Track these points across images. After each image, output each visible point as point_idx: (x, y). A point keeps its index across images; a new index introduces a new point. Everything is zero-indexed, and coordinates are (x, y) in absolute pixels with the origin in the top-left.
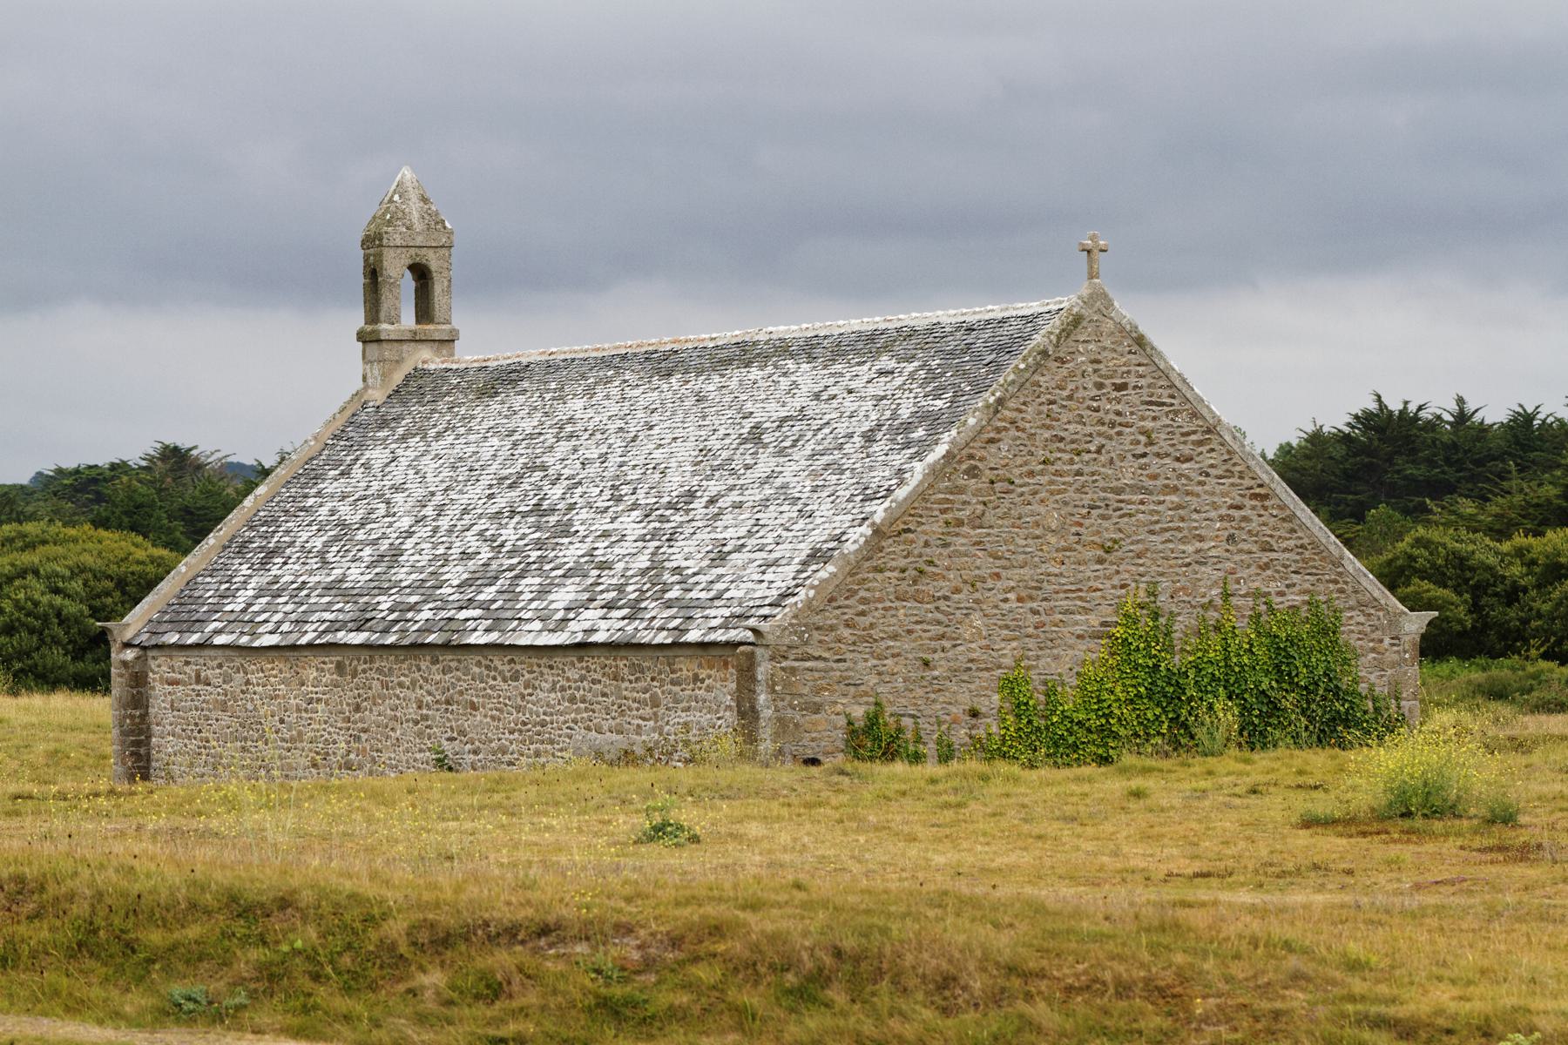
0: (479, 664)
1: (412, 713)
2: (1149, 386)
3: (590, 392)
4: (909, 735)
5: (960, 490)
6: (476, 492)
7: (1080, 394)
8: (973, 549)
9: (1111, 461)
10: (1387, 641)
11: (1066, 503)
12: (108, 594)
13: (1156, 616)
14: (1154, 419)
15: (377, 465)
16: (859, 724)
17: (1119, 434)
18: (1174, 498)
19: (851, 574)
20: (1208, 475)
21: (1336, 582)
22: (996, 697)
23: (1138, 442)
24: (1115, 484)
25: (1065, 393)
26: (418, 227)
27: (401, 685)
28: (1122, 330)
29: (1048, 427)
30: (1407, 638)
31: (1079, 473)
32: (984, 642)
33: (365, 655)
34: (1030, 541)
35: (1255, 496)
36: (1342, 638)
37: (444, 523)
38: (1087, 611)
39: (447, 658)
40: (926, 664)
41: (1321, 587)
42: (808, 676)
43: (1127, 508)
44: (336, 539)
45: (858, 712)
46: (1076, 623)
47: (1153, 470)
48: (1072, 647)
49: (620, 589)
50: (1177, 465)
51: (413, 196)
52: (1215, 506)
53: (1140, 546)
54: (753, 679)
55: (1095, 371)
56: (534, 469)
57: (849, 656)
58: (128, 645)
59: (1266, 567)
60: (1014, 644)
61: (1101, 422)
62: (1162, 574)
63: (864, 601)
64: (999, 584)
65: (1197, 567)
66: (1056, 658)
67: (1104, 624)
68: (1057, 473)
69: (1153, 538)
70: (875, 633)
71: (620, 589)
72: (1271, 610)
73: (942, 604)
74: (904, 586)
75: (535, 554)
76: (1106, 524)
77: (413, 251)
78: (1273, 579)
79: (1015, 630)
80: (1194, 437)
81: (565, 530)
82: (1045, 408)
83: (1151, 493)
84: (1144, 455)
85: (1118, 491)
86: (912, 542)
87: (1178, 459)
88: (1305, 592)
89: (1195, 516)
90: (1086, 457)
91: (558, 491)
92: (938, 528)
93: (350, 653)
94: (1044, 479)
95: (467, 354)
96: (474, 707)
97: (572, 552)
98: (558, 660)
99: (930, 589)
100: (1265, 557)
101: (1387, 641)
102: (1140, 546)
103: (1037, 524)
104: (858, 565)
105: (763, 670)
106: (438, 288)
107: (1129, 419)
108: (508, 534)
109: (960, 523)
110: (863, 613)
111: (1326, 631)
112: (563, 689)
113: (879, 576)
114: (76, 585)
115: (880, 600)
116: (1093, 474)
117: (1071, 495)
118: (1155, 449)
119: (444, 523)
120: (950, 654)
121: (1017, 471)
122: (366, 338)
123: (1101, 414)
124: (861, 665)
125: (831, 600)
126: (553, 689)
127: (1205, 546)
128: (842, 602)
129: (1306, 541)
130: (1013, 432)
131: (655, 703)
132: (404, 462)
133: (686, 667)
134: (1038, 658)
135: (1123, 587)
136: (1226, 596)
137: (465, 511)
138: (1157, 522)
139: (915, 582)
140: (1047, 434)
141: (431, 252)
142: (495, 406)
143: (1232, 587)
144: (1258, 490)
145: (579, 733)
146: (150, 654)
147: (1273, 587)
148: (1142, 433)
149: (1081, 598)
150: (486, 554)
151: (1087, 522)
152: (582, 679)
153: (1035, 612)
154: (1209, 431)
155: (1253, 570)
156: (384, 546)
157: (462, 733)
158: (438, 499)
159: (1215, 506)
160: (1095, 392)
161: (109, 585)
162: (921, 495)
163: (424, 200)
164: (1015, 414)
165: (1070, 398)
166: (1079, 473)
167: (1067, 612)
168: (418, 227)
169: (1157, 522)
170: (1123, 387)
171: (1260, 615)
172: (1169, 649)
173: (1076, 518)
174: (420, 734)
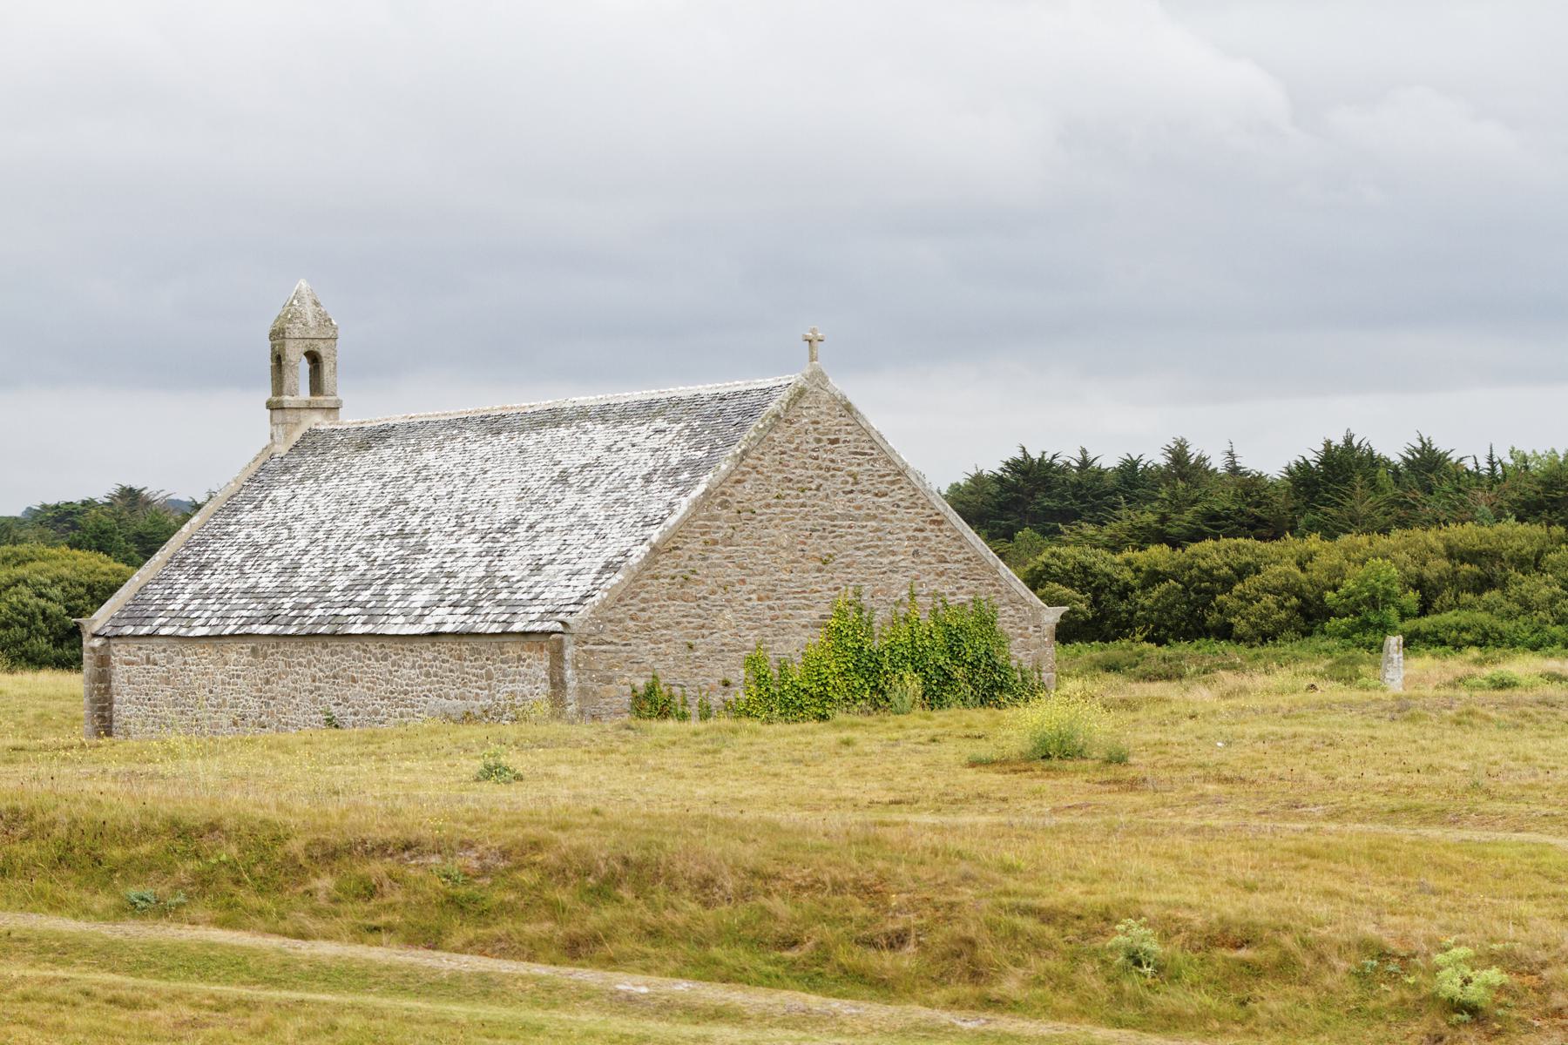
0: (358, 648)
1: (308, 684)
3: (440, 446)
4: (678, 700)
5: (716, 518)
6: (355, 521)
7: (805, 446)
8: (725, 562)
10: (1031, 629)
12: (80, 597)
13: (860, 611)
15: (281, 501)
16: (641, 692)
18: (874, 524)
19: (635, 580)
22: (742, 672)
26: (312, 323)
27: (300, 664)
28: (835, 399)
31: (803, 505)
33: (273, 641)
35: (933, 522)
36: (998, 627)
37: (332, 544)
39: (334, 643)
40: (691, 647)
41: (982, 589)
42: (603, 656)
43: (839, 531)
44: (251, 556)
45: (640, 683)
49: (463, 592)
52: (904, 529)
54: (562, 659)
56: (399, 503)
58: (95, 635)
59: (942, 574)
63: (644, 600)
64: (744, 588)
66: (787, 642)
67: (822, 617)
70: (653, 624)
71: (463, 592)
72: (946, 607)
73: (702, 602)
74: (673, 590)
75: (399, 567)
76: (823, 543)
79: (756, 623)
81: (422, 549)
85: (832, 518)
90: (809, 493)
91: (416, 520)
92: (699, 546)
93: (261, 641)
94: (778, 510)
95: (349, 418)
96: (354, 680)
97: (426, 565)
98: (417, 645)
101: (1031, 629)
103: (773, 543)
104: (640, 574)
105: (570, 652)
106: (326, 369)
107: (840, 465)
108: (379, 552)
109: (715, 543)
110: (643, 610)
111: (986, 622)
112: (420, 667)
113: (655, 582)
114: (56, 592)
115: (656, 600)
117: (797, 521)
118: (859, 487)
119: (332, 544)
122: (273, 407)
124: (642, 648)
126: (413, 667)
127: (897, 559)
128: (627, 601)
130: (754, 475)
131: (489, 677)
132: (301, 499)
133: (512, 650)
136: (913, 596)
137: (347, 535)
140: (780, 477)
142: (369, 456)
143: (917, 589)
145: (433, 699)
146: (112, 642)
147: (947, 589)
150: (363, 567)
152: (435, 659)
155: (932, 576)
156: (287, 561)
157: (346, 700)
158: (327, 525)
159: (904, 529)
160: (815, 445)
161: (82, 590)
162: (686, 522)
163: (316, 304)
165: (796, 449)
166: (803, 505)
168: (312, 323)
170: (833, 442)
172: (871, 635)
173: (802, 539)
174: (314, 701)
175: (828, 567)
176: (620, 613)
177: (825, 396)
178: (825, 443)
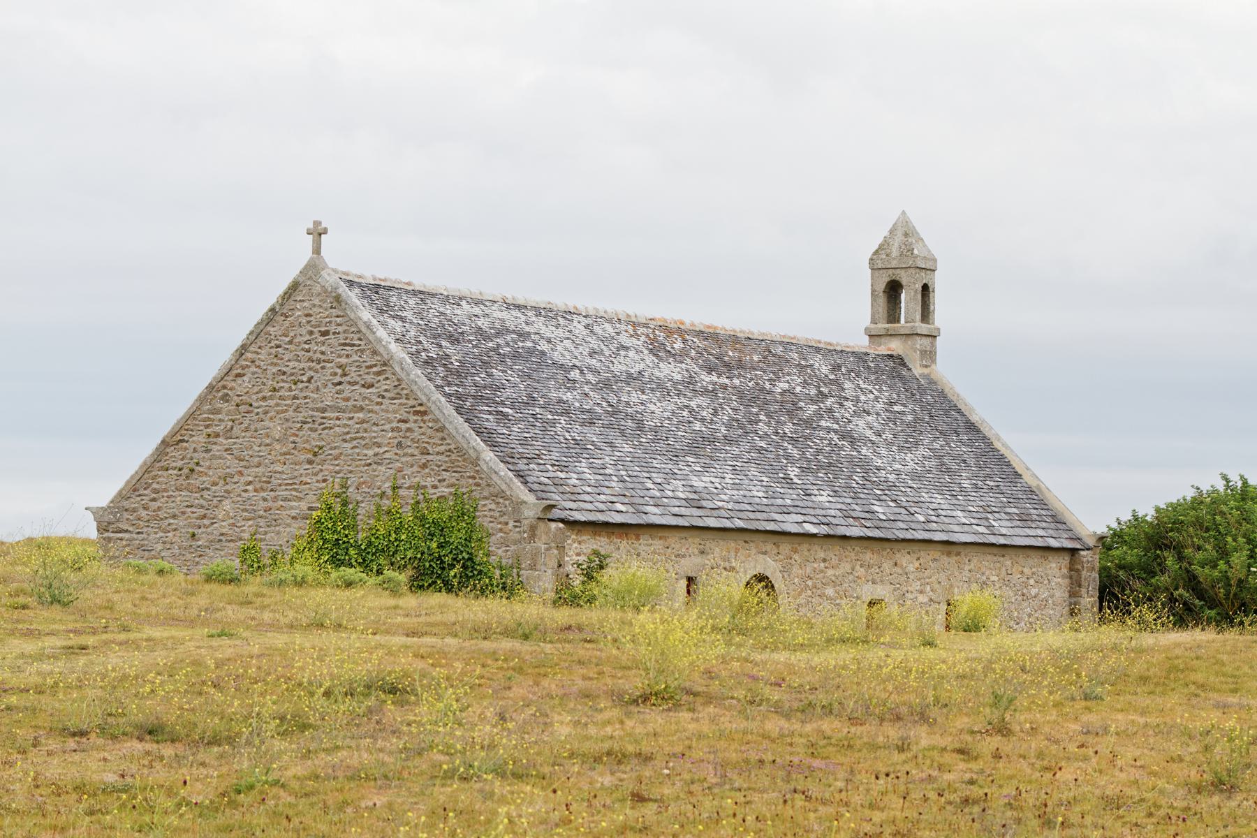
2: (345, 332)
5: (218, 411)
7: (298, 339)
9: (318, 389)
10: (511, 524)
11: (287, 420)
13: (345, 503)
14: (348, 356)
17: (323, 368)
18: (361, 415)
20: (383, 397)
21: (474, 478)
23: (336, 374)
24: (320, 405)
25: (287, 339)
26: (895, 253)
29: (276, 365)
30: (526, 522)
31: (295, 398)
32: (232, 521)
34: (263, 448)
38: (300, 499)
41: (463, 482)
43: (329, 423)
46: (292, 508)
47: (346, 394)
48: (289, 525)
50: (363, 390)
51: (900, 233)
53: (337, 451)
55: (309, 322)
57: (145, 530)
59: (424, 466)
60: (251, 523)
61: (311, 360)
62: (351, 472)
63: (156, 491)
64: (243, 479)
65: (374, 466)
66: (278, 533)
67: (310, 509)
68: (281, 398)
69: (346, 445)
70: (162, 514)
73: (205, 494)
74: (181, 481)
76: (314, 435)
77: (890, 272)
78: (429, 475)
80: (375, 369)
82: (273, 351)
83: (344, 412)
84: (340, 383)
85: (324, 410)
86: (186, 449)
87: (363, 386)
88: (453, 485)
89: (375, 428)
90: (301, 385)
92: (202, 439)
94: (272, 403)
99: (197, 483)
100: (424, 459)
101: (511, 524)
102: (337, 451)
104: (152, 466)
109: (218, 435)
113: (165, 473)
115: (166, 490)
116: (305, 398)
118: (348, 379)
120: (209, 530)
121: (254, 397)
123: (311, 354)
125: (135, 490)
128: (141, 492)
129: (452, 447)
130: (253, 369)
134: (266, 533)
135: (324, 481)
136: (394, 488)
138: (348, 433)
139: (187, 477)
140: (275, 370)
141: (902, 272)
143: (400, 482)
144: (419, 408)
148: (340, 367)
149: (296, 490)
151: (301, 433)
153: (265, 500)
154: (385, 364)
155: (415, 468)
164: (254, 356)
165: (290, 342)
166: (295, 398)
167: (285, 500)
169: (348, 433)
171: (418, 503)
172: (354, 527)
175: (317, 460)
176: (133, 503)
177: (317, 289)
178: (317, 335)
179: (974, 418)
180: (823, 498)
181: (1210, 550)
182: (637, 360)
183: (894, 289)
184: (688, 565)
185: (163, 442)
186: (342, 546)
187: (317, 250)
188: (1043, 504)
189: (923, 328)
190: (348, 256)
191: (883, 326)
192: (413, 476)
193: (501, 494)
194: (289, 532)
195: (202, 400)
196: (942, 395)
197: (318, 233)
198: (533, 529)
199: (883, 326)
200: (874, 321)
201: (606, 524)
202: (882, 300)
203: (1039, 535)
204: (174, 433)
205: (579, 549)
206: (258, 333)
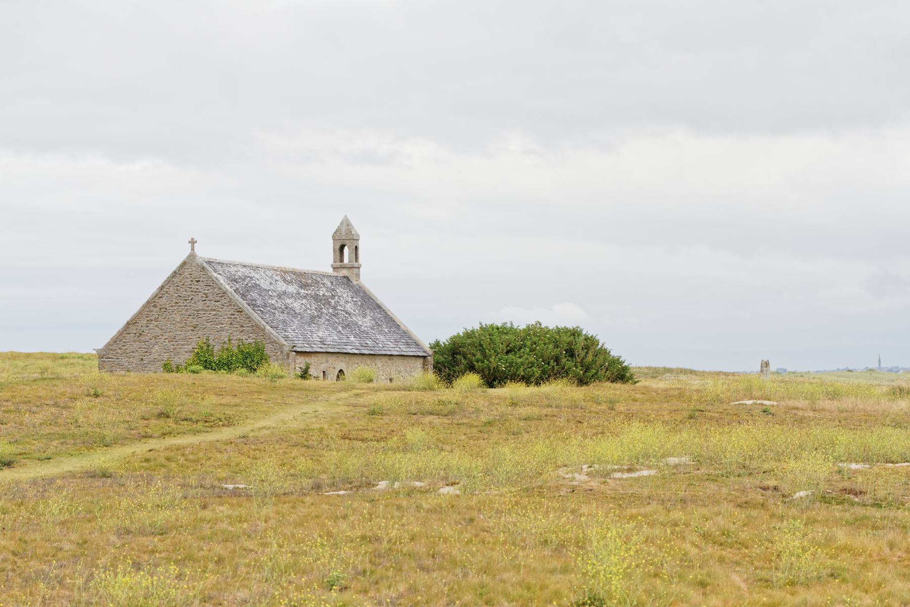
13: (208, 346)
26: (344, 233)
51: (345, 225)
79: (168, 350)
111: (259, 350)
117: (184, 312)
147: (244, 337)
168: (344, 233)
172: (212, 355)
179: (378, 302)
180: (352, 339)
181: (479, 356)
182: (282, 287)
183: (342, 247)
184: (323, 367)
185: (128, 323)
186: (207, 361)
187: (193, 249)
188: (410, 338)
189: (356, 265)
190: (204, 253)
191: (339, 264)
192: (237, 335)
193: (274, 342)
194: (184, 357)
195: (144, 306)
196: (365, 292)
197: (193, 242)
198: (288, 355)
199: (339, 264)
200: (335, 262)
201: (306, 352)
202: (338, 253)
203: (411, 351)
204: (132, 320)
205: (301, 361)
206: (169, 281)
